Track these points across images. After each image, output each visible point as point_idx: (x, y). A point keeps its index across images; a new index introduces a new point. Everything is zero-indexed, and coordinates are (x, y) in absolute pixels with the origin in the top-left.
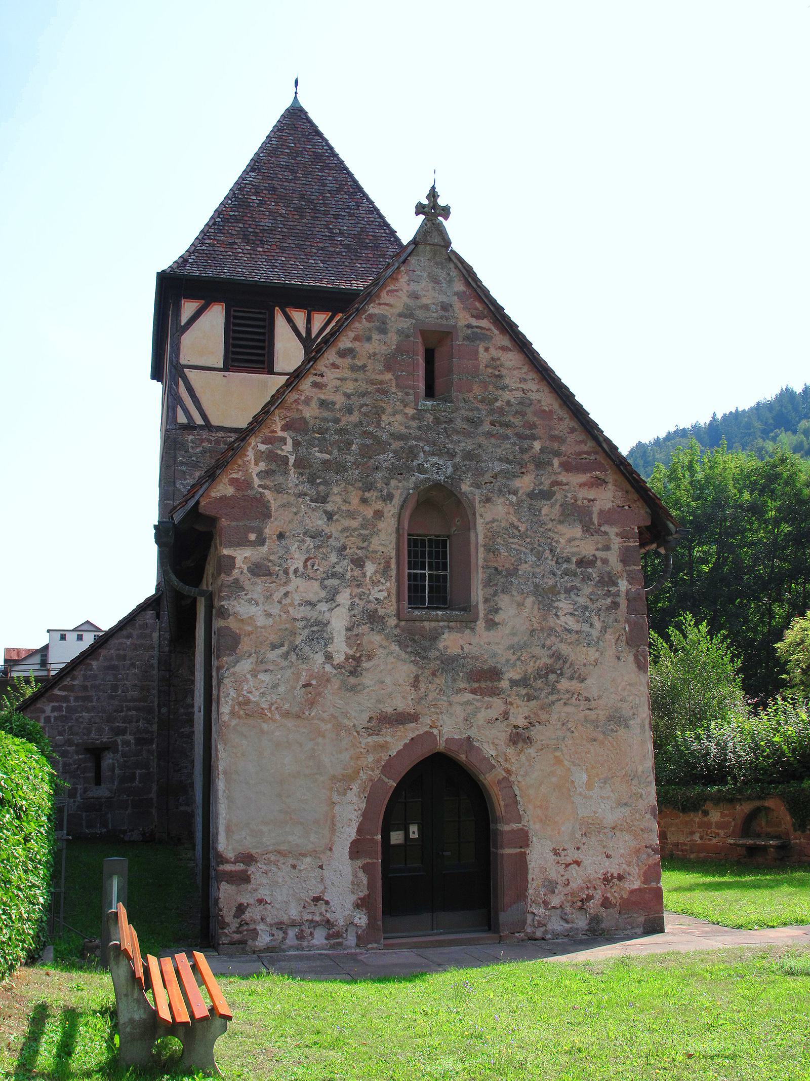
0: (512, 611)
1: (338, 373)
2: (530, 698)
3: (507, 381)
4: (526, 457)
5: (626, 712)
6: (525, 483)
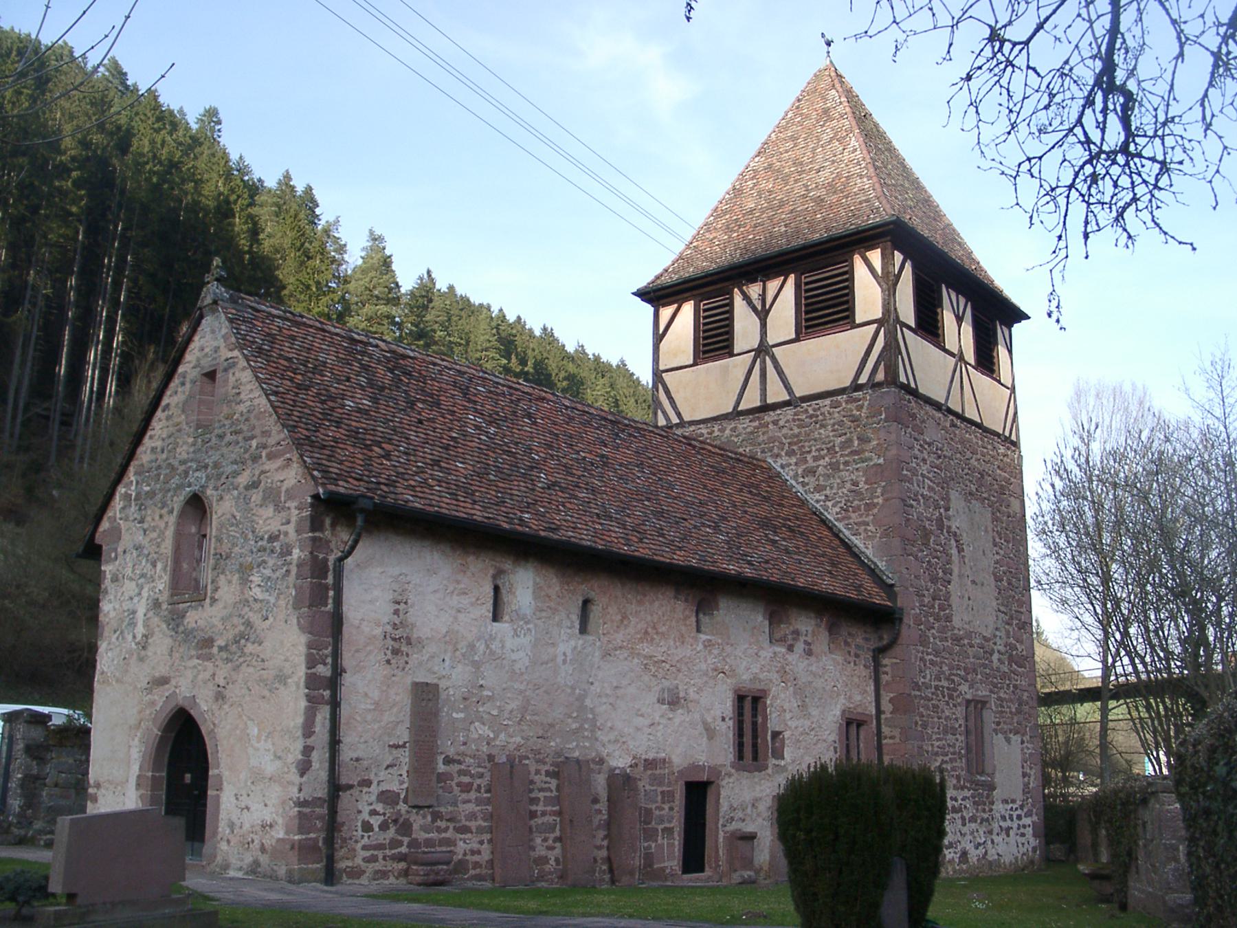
0: (226, 589)
1: (161, 425)
2: (228, 660)
3: (242, 396)
4: (247, 456)
5: (288, 670)
6: (243, 480)
